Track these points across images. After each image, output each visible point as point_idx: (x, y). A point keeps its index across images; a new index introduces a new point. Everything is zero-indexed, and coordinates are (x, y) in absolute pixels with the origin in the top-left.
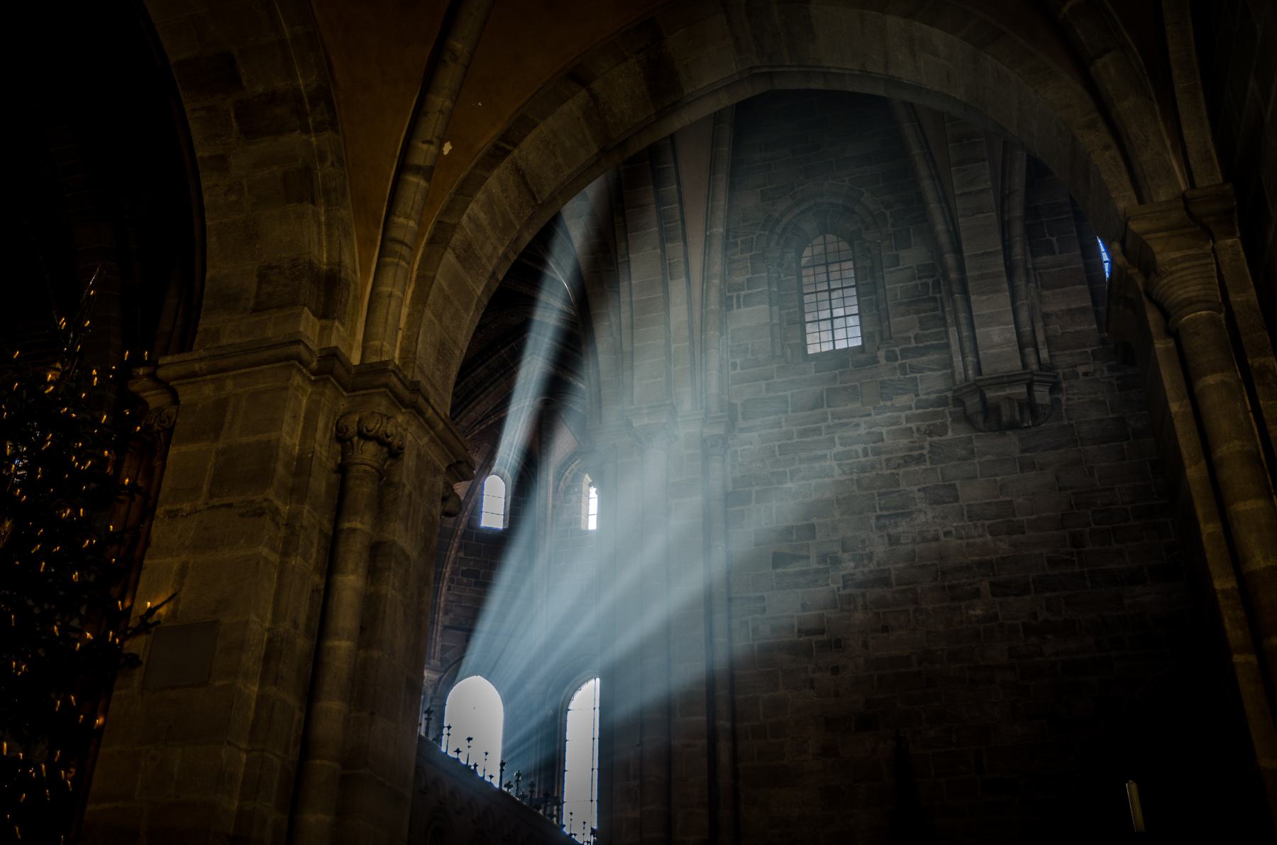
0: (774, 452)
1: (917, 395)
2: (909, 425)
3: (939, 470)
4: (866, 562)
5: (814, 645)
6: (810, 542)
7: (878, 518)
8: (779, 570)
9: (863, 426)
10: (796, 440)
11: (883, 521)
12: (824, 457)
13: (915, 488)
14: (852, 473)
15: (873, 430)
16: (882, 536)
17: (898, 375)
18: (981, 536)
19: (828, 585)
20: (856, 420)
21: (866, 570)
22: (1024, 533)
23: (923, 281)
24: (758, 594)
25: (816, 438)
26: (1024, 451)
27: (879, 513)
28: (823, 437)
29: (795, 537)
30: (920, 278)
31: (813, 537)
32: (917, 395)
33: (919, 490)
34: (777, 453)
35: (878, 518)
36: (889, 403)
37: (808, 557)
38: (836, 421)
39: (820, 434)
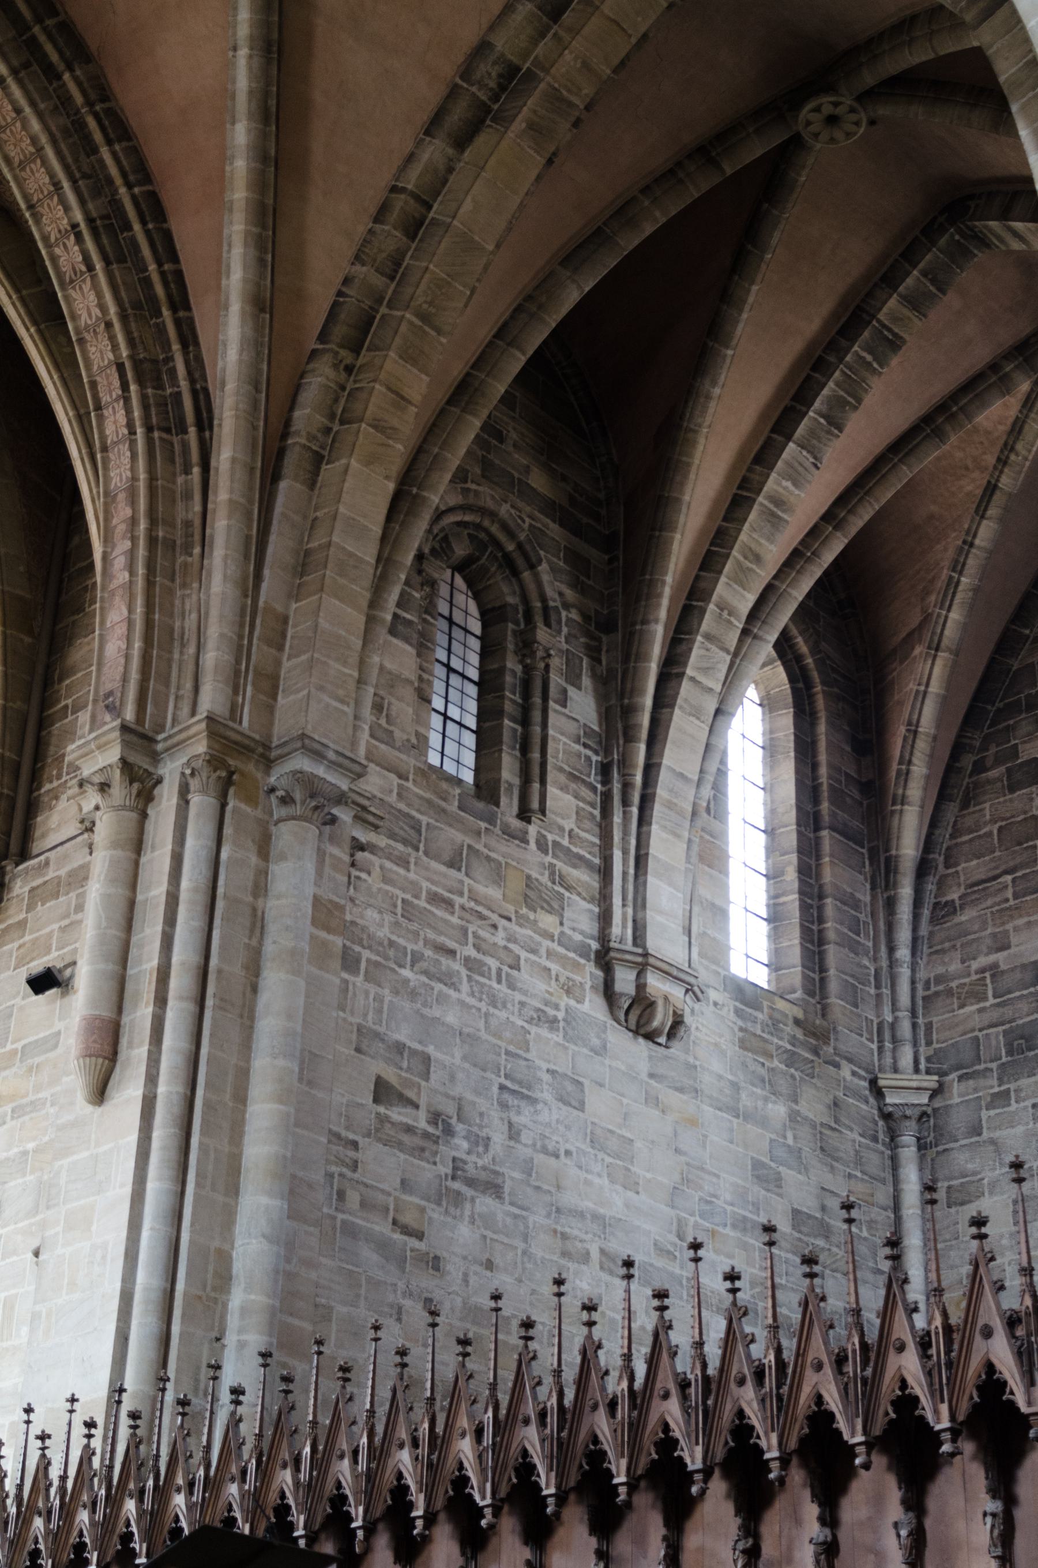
0: (395, 906)
1: (561, 924)
2: (549, 964)
3: (570, 1052)
4: (481, 1149)
5: (408, 1253)
6: (423, 1083)
7: (502, 1087)
8: (382, 1109)
9: (501, 934)
10: (422, 903)
11: (506, 1096)
12: (452, 953)
13: (545, 1066)
14: (481, 1000)
15: (511, 946)
16: (502, 1119)
17: (545, 879)
18: (599, 1175)
19: (435, 1163)
20: (495, 918)
21: (480, 1163)
22: (638, 1193)
23: (589, 753)
24: (351, 1136)
25: (448, 917)
26: (651, 1076)
27: (502, 1080)
28: (455, 920)
29: (405, 1065)
30: (585, 745)
31: (426, 1076)
32: (561, 924)
33: (548, 1071)
34: (399, 910)
35: (502, 1087)
36: (532, 916)
37: (417, 1107)
38: (472, 904)
39: (453, 913)
